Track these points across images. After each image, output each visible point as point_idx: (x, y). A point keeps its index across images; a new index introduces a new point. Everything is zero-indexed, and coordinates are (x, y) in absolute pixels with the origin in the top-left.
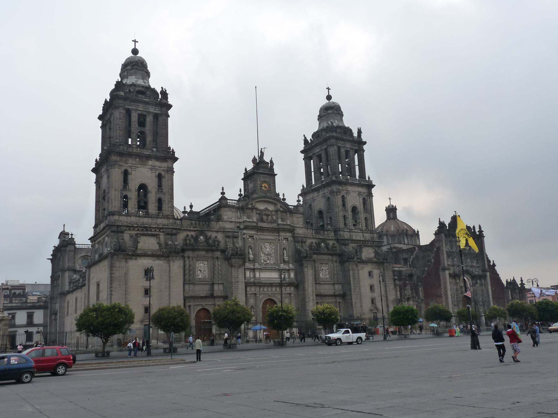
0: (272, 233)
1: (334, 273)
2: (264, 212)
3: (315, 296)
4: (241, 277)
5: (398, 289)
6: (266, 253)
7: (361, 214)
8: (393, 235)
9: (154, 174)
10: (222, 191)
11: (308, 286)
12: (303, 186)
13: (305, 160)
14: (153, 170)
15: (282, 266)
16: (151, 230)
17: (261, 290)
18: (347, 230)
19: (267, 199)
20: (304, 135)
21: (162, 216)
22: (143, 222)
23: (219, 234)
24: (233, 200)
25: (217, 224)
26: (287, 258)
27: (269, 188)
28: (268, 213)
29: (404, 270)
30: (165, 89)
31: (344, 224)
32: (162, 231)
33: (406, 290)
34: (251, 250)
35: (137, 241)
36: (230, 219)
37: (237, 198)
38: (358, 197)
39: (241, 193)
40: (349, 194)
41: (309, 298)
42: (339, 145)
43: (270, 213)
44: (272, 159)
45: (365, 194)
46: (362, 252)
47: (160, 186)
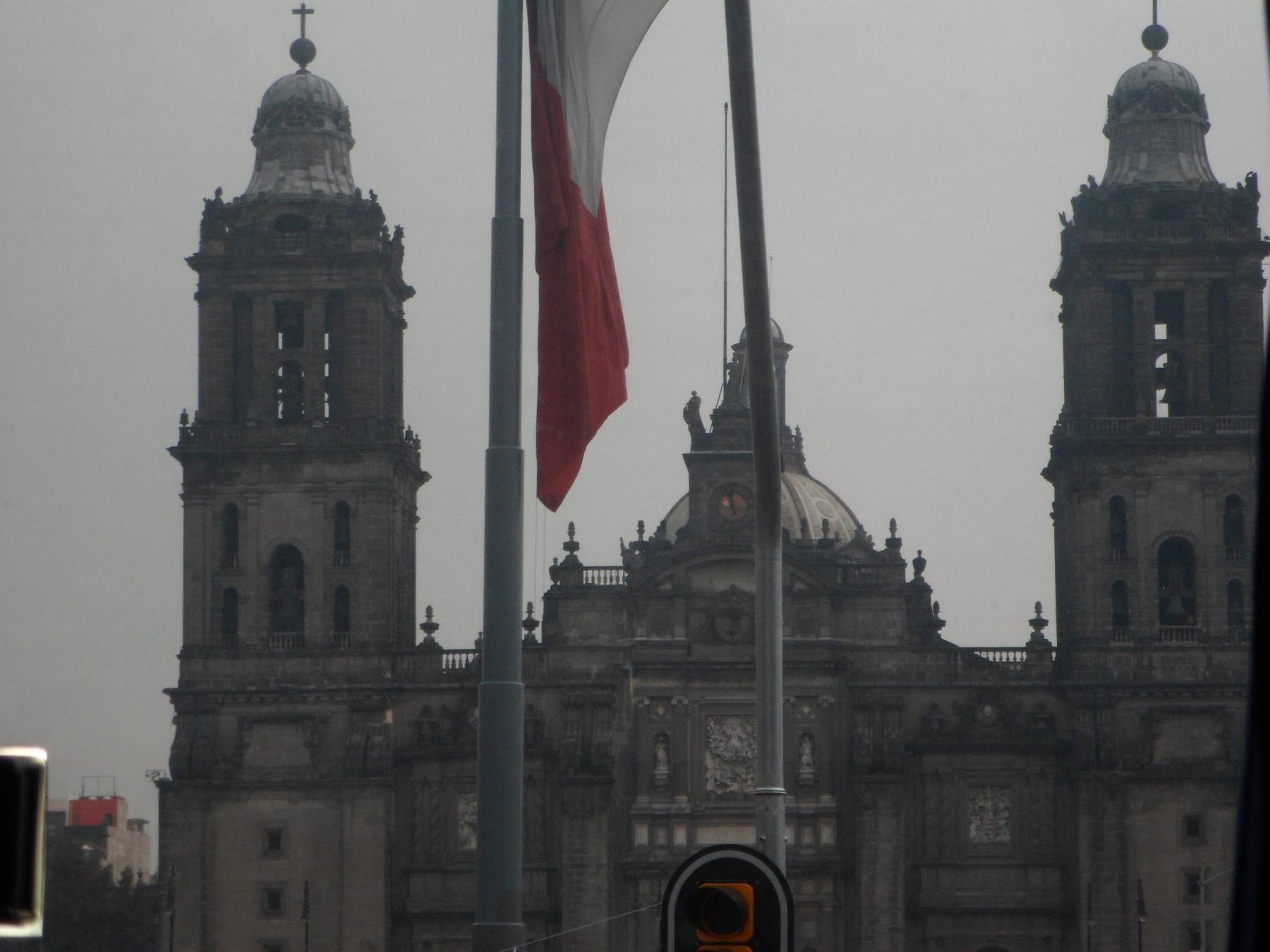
3: (900, 916)
4: (596, 849)
6: (728, 755)
10: (567, 539)
16: (304, 698)
19: (731, 556)
21: (349, 646)
24: (605, 568)
30: (371, 192)
31: (1110, 619)
34: (667, 750)
36: (590, 637)
39: (641, 537)
42: (1122, 277)
47: (342, 544)
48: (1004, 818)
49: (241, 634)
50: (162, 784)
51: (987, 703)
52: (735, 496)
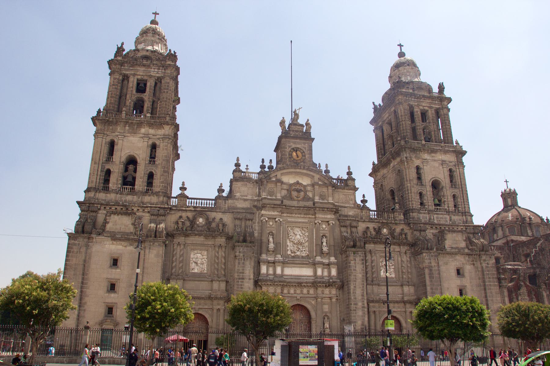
0: (305, 214)
1: (402, 271)
2: (294, 187)
3: (365, 301)
4: (249, 272)
5: (506, 293)
6: (296, 242)
7: (446, 189)
8: (511, 226)
9: (146, 143)
10: (236, 162)
11: (355, 287)
12: (374, 164)
13: (375, 131)
14: (145, 138)
15: (318, 259)
17: (285, 291)
18: (425, 212)
20: (373, 103)
22: (126, 201)
23: (227, 215)
25: (225, 203)
26: (328, 248)
27: (303, 156)
28: (299, 188)
29: (521, 269)
30: (174, 51)
31: (419, 203)
32: (147, 211)
33: (520, 295)
34: (273, 238)
35: (106, 220)
36: (245, 196)
37: (259, 170)
38: (441, 167)
40: (427, 164)
41: (356, 304)
42: (411, 103)
43: (302, 188)
44: (308, 120)
45: (451, 164)
46: (445, 240)
47: (153, 157)
48: (393, 269)
49: (110, 185)
50: (70, 235)
51: (384, 228)
52: (298, 152)
